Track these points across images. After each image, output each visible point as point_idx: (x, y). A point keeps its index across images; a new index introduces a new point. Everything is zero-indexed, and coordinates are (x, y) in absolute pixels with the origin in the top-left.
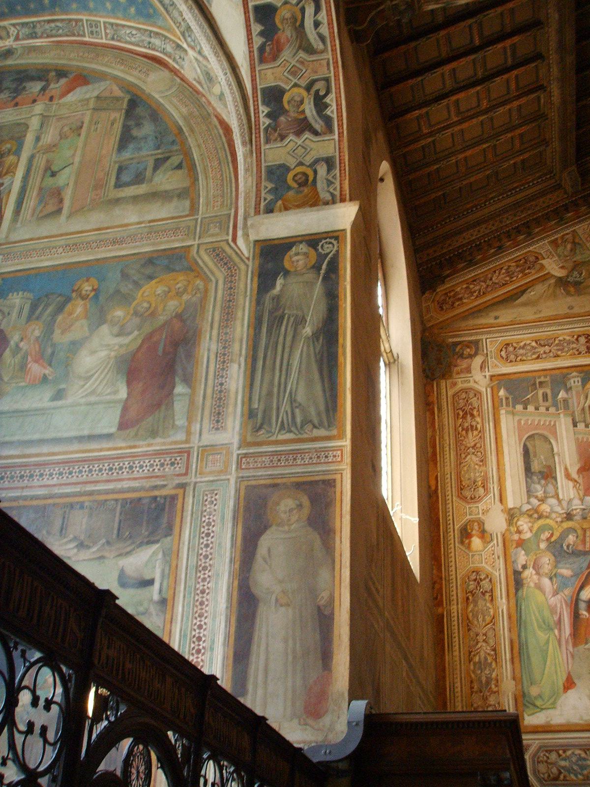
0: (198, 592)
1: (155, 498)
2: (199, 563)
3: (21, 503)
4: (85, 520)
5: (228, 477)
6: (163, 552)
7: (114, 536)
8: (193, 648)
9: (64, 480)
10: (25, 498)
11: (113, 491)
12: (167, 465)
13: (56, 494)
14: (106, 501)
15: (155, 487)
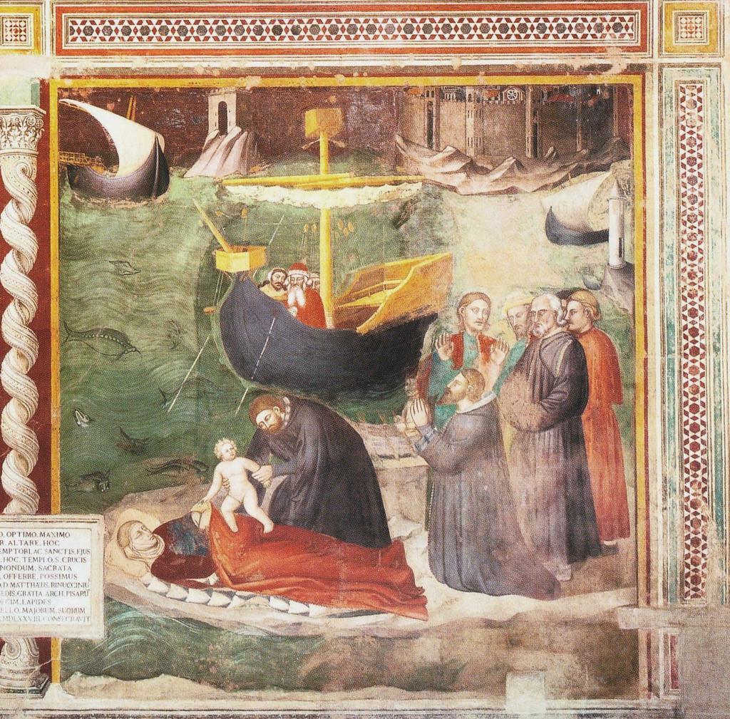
0: (685, 256)
1: (593, 88)
2: (683, 209)
3: (340, 80)
4: (471, 121)
5: (719, 60)
6: (619, 186)
7: (529, 155)
8: (686, 347)
9: (418, 43)
10: (348, 73)
11: (512, 71)
12: (608, 28)
13: (406, 67)
14: (504, 87)
15: (591, 69)
